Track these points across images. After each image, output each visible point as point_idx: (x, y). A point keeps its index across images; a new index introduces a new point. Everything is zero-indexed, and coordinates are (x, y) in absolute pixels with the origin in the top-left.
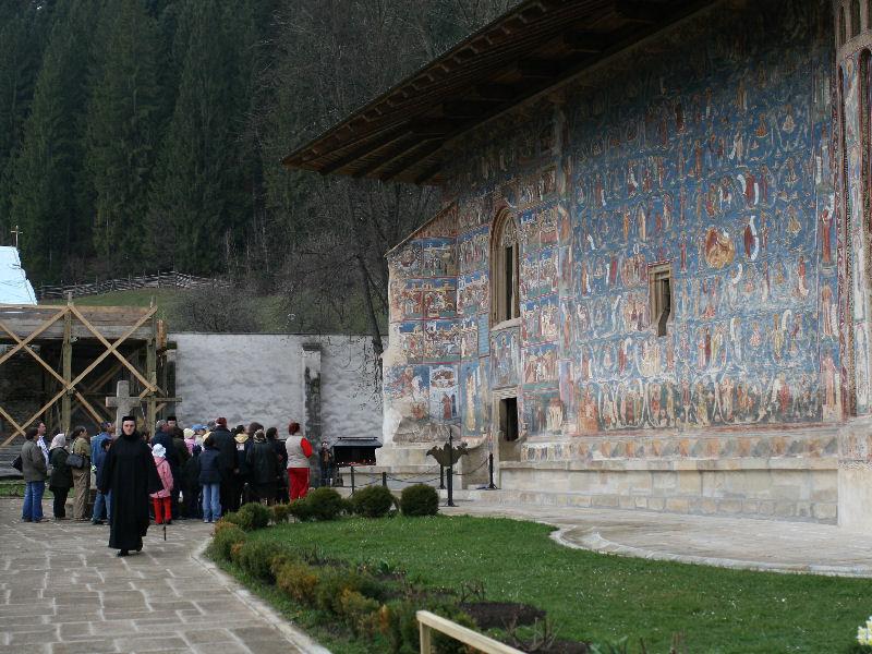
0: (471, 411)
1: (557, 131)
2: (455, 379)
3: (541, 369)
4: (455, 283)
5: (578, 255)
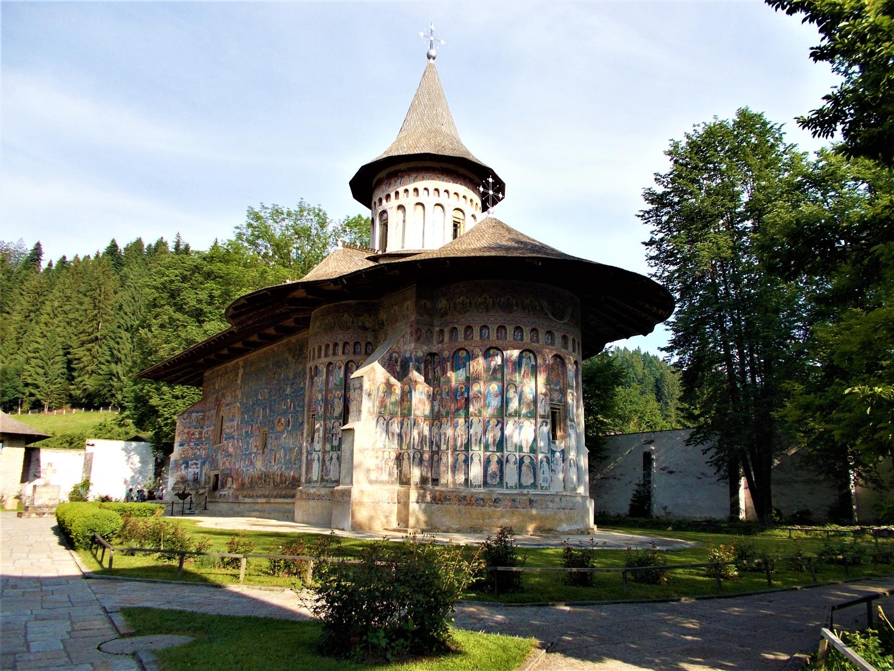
0: (203, 479)
1: (240, 375)
2: (199, 466)
3: (227, 463)
4: (202, 428)
5: (241, 423)
